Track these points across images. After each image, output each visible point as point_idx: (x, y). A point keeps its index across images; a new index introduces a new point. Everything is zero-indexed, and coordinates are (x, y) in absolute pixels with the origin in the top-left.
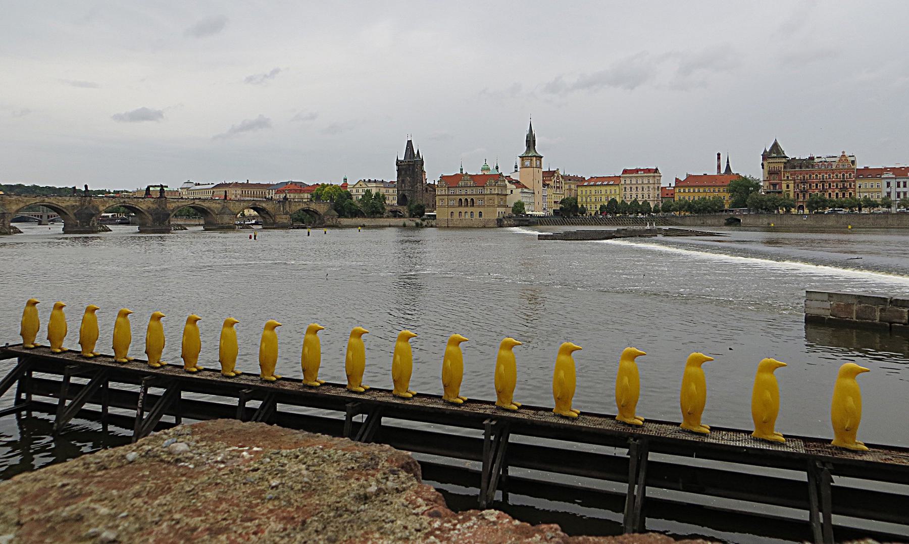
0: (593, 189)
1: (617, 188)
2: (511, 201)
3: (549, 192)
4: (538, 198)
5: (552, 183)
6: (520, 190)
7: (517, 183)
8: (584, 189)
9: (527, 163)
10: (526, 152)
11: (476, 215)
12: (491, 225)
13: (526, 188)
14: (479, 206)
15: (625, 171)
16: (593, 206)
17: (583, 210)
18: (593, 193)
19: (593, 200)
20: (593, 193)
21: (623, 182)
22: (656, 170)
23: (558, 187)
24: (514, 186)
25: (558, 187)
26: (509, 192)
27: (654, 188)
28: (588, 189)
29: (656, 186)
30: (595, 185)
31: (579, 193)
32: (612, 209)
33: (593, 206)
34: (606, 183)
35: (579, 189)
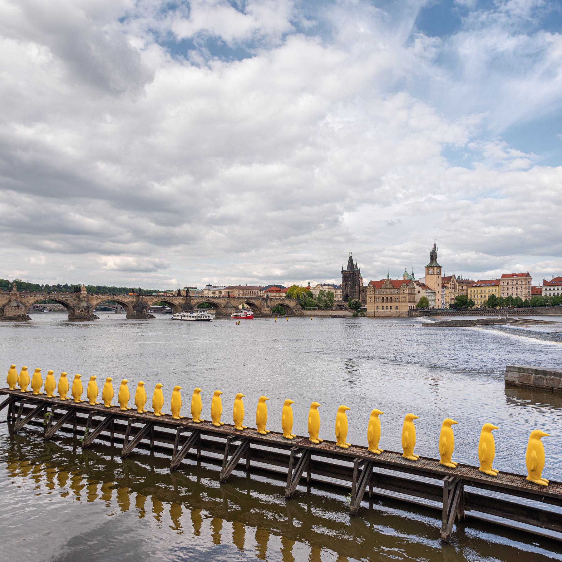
0: (479, 289)
1: (497, 288)
2: (418, 298)
3: (447, 291)
4: (438, 296)
5: (448, 285)
6: (424, 291)
7: (423, 286)
8: (472, 289)
9: (431, 271)
10: (430, 264)
11: (394, 308)
12: (404, 315)
13: (429, 289)
14: (395, 302)
15: (504, 276)
16: (479, 301)
17: (472, 303)
18: (479, 292)
19: (479, 297)
20: (479, 292)
21: (501, 284)
22: (528, 274)
23: (454, 288)
24: (420, 288)
25: (454, 288)
26: (416, 292)
27: (526, 288)
28: (476, 289)
29: (527, 286)
30: (480, 286)
31: (469, 292)
32: (493, 302)
33: (479, 301)
34: (489, 284)
35: (469, 290)
